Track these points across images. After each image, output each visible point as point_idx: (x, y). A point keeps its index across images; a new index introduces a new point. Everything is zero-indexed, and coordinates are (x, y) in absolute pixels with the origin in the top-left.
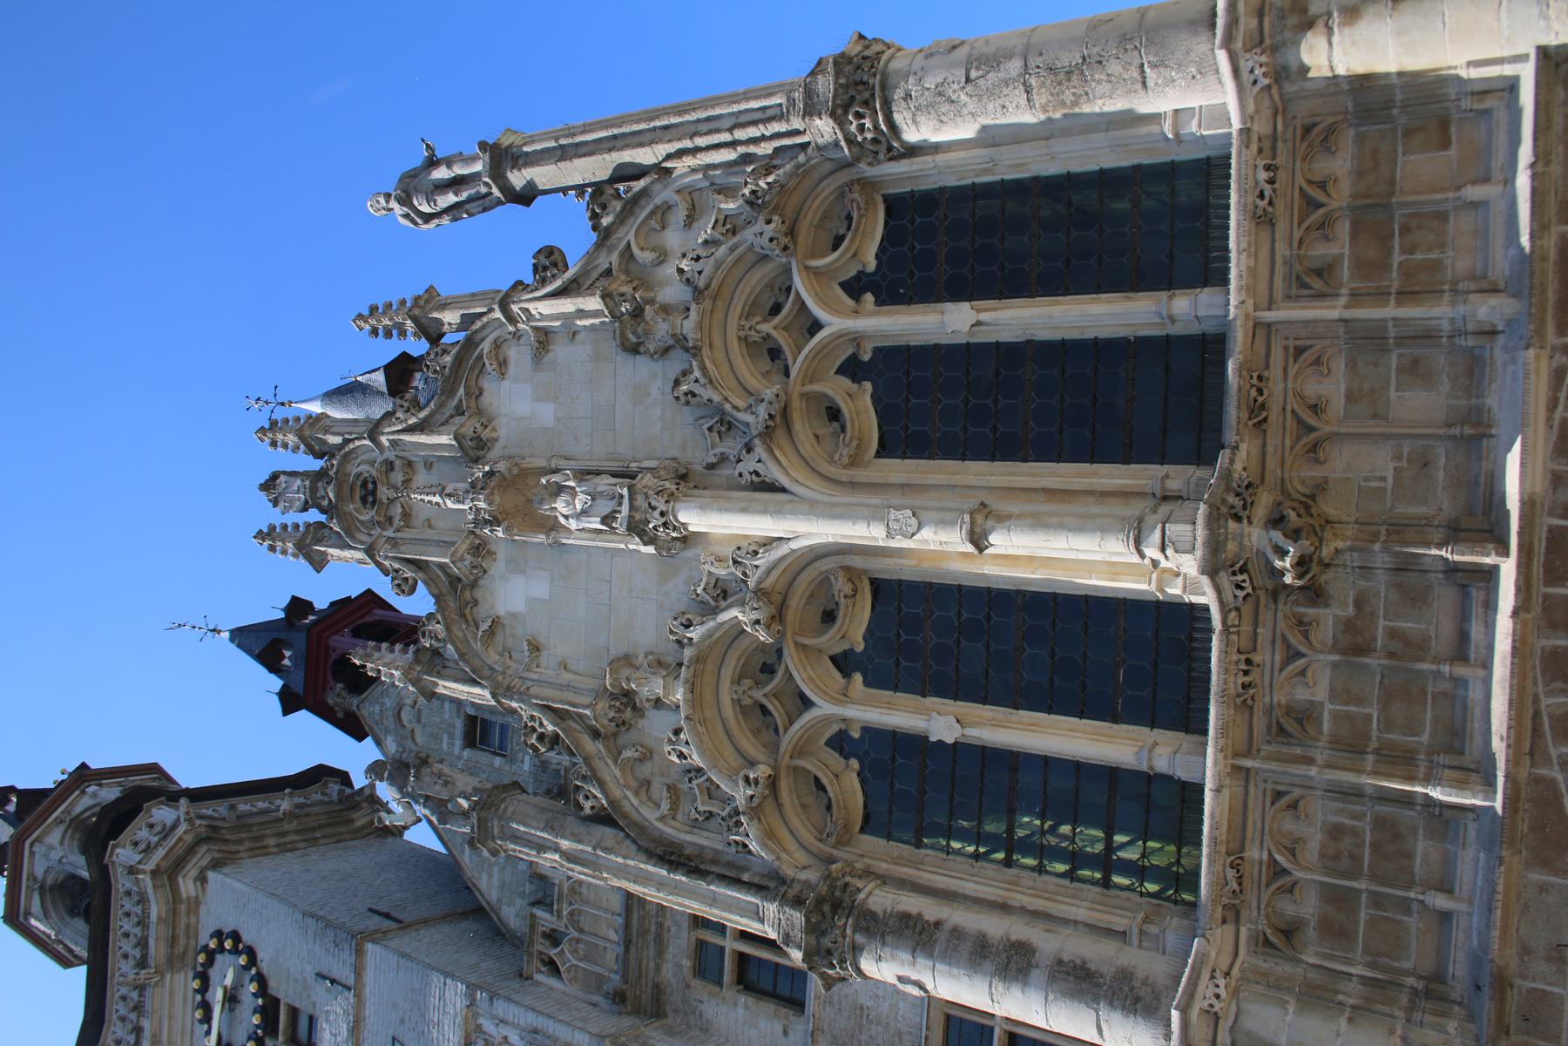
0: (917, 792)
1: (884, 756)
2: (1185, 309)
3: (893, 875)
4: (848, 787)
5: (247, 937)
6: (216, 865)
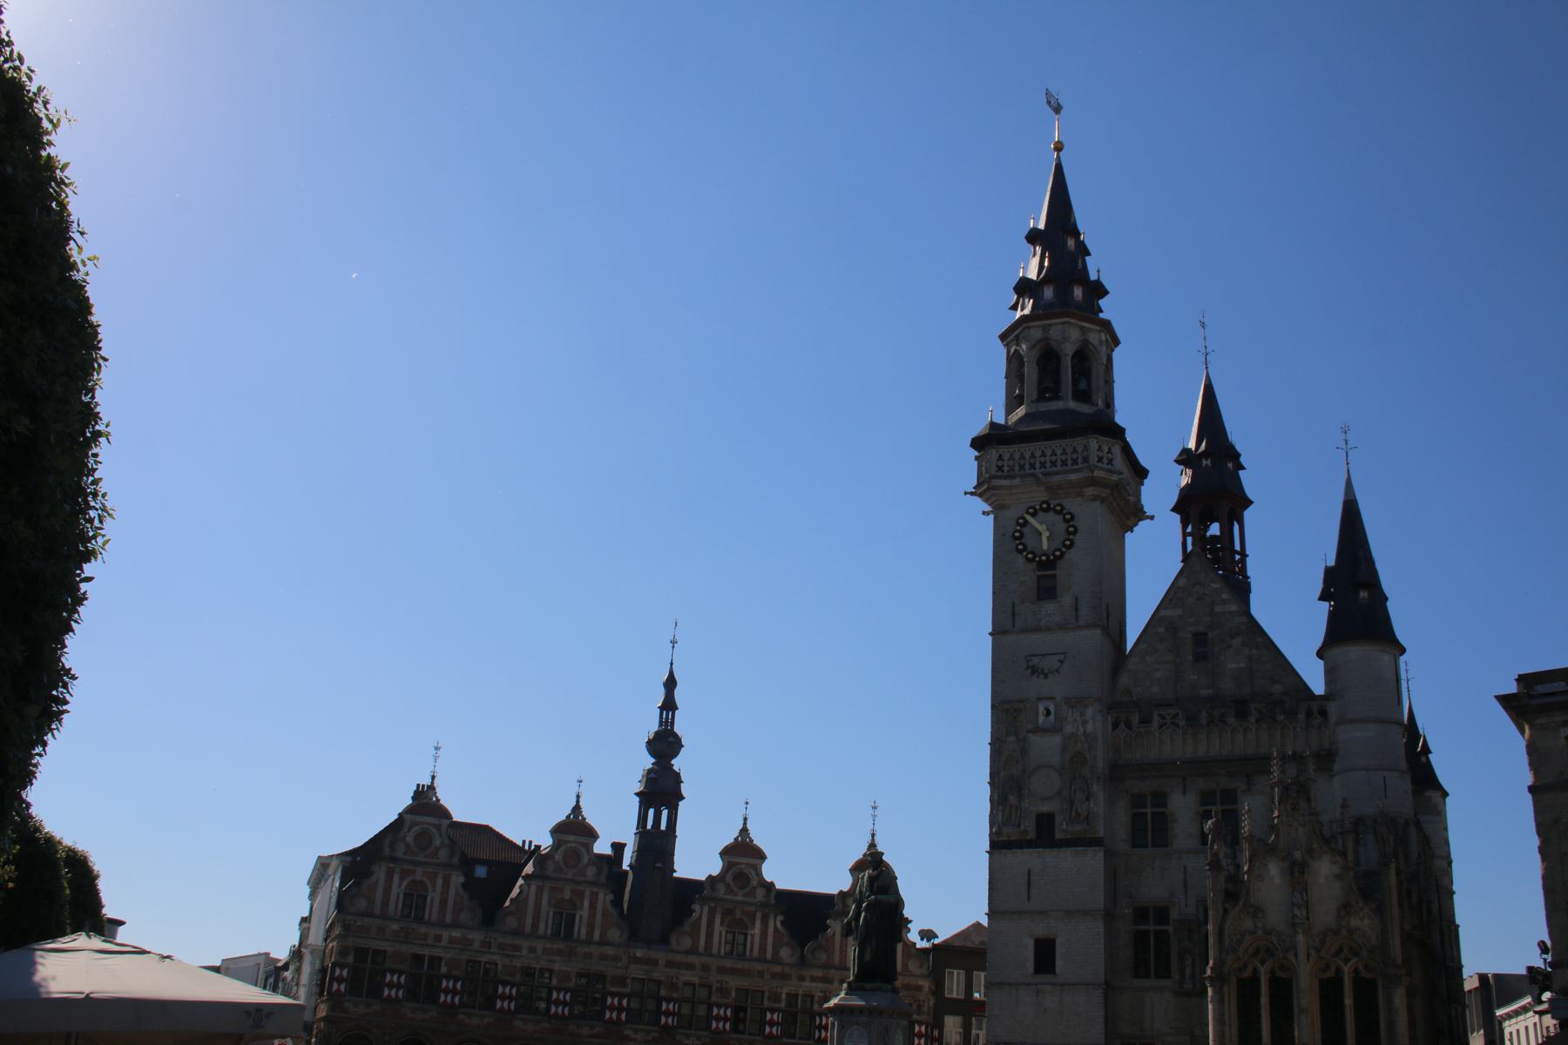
0: (1248, 988)
1: (1255, 979)
4: (1247, 974)
5: (1078, 539)
6: (1103, 500)
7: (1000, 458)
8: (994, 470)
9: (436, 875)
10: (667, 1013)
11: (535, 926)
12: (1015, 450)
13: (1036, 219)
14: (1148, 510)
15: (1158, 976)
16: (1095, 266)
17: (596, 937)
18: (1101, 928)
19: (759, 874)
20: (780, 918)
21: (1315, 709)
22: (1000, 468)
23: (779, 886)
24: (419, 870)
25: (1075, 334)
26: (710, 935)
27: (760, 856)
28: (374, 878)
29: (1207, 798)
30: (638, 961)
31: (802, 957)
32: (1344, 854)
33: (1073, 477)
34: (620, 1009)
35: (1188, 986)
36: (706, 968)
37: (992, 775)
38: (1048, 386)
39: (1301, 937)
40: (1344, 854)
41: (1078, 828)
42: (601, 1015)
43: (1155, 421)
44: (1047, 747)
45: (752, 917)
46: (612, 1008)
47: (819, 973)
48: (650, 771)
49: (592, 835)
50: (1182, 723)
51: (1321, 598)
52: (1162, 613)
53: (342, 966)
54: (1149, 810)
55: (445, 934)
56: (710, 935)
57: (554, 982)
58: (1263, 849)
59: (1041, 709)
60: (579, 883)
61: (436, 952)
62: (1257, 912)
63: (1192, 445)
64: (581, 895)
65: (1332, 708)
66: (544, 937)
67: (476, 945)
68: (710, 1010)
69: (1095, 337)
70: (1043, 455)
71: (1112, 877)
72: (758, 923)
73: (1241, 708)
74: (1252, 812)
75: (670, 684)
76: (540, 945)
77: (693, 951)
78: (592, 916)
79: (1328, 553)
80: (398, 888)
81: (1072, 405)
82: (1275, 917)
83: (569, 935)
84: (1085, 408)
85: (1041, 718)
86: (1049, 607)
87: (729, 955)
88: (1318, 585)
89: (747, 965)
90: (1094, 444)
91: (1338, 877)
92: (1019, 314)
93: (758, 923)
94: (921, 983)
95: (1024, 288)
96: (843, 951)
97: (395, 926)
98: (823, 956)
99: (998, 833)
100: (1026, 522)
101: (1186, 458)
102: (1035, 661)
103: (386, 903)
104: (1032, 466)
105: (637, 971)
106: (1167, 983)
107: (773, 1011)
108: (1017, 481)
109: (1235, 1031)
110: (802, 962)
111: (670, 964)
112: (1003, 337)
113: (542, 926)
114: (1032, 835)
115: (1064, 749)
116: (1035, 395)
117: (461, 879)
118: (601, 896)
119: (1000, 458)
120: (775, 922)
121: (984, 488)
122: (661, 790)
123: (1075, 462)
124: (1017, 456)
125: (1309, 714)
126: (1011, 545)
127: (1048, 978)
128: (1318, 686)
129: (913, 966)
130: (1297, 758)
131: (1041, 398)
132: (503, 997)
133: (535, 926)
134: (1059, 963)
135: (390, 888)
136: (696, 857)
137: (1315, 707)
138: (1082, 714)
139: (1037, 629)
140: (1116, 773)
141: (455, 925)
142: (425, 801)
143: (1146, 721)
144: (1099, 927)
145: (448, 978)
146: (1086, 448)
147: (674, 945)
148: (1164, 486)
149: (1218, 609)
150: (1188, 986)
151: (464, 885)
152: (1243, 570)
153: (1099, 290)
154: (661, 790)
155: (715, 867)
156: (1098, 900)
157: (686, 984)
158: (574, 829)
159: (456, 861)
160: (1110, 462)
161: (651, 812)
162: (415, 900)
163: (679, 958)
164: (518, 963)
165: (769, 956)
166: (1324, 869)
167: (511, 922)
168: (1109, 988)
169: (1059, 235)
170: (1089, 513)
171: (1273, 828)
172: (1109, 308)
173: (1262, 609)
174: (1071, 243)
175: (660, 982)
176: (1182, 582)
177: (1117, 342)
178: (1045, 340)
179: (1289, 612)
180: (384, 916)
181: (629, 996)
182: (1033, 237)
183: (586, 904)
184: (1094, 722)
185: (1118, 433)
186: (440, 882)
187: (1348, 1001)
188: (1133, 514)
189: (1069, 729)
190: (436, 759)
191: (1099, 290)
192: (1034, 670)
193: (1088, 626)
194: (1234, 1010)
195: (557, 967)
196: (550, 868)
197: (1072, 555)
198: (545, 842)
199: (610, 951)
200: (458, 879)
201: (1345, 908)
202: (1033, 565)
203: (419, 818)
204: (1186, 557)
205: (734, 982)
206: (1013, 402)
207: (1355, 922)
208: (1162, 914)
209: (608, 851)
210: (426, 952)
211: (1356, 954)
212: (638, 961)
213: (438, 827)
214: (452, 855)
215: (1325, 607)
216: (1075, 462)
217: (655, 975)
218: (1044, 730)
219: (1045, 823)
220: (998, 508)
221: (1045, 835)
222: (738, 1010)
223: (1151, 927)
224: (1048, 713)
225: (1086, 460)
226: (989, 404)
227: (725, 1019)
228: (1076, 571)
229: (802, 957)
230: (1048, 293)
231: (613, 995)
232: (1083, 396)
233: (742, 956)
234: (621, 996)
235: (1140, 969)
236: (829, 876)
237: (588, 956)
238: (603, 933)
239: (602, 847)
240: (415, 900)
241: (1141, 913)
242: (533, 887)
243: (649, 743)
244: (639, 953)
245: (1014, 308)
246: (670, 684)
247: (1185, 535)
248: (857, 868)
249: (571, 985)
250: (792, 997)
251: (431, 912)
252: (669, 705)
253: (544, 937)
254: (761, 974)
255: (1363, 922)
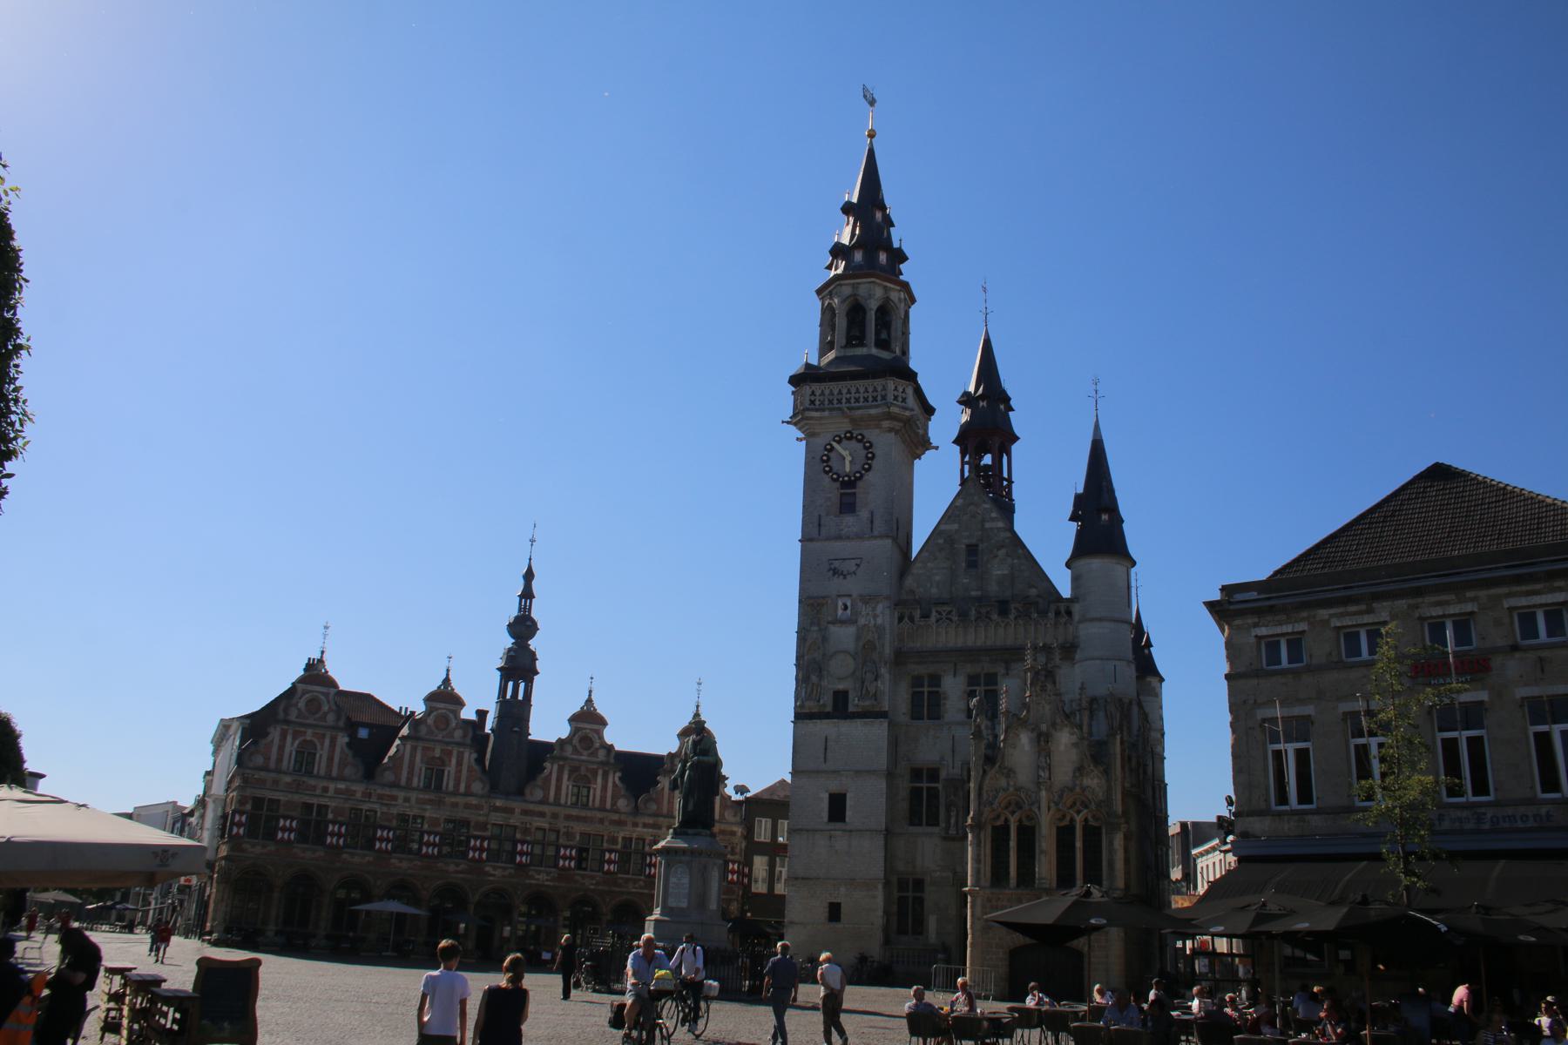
0: (1000, 834)
1: (1006, 827)
2: (1079, 882)
3: (987, 835)
4: (999, 823)
5: (874, 463)
6: (897, 432)
7: (813, 393)
8: (807, 404)
9: (323, 736)
10: (522, 853)
11: (409, 779)
12: (827, 387)
13: (850, 194)
14: (934, 441)
15: (928, 824)
16: (897, 236)
17: (462, 788)
18: (884, 785)
19: (601, 738)
20: (618, 774)
21: (1062, 608)
22: (812, 402)
23: (618, 747)
24: (309, 731)
25: (879, 292)
26: (558, 788)
27: (604, 723)
28: (270, 738)
29: (973, 680)
30: (496, 809)
31: (636, 807)
32: (1080, 727)
33: (873, 412)
34: (481, 850)
35: (952, 832)
36: (555, 816)
37: (798, 659)
38: (855, 335)
39: (1043, 793)
40: (1080, 727)
41: (867, 703)
42: (464, 855)
43: (942, 367)
44: (843, 636)
45: (595, 774)
46: (475, 849)
47: (650, 821)
48: (510, 650)
49: (459, 703)
50: (955, 618)
51: (1071, 519)
52: (942, 527)
53: (241, 813)
54: (926, 689)
55: (332, 786)
56: (558, 788)
57: (426, 827)
58: (1016, 722)
59: (840, 603)
60: (448, 743)
61: (323, 801)
62: (1009, 773)
63: (971, 389)
64: (450, 753)
65: (1076, 609)
66: (417, 789)
67: (359, 795)
68: (558, 851)
69: (894, 296)
70: (849, 392)
71: (894, 743)
72: (599, 780)
73: (1003, 607)
74: (1009, 691)
75: (529, 576)
76: (413, 796)
77: (541, 802)
78: (459, 771)
79: (1077, 481)
80: (291, 746)
81: (874, 351)
82: (1024, 777)
83: (439, 788)
84: (885, 355)
85: (840, 612)
86: (849, 520)
87: (574, 805)
88: (1069, 508)
89: (589, 814)
90: (891, 384)
91: (1075, 745)
92: (833, 273)
93: (599, 780)
94: (735, 829)
95: (838, 251)
96: (671, 803)
97: (288, 779)
98: (654, 807)
99: (802, 706)
100: (832, 448)
101: (966, 400)
102: (836, 564)
103: (280, 760)
104: (840, 401)
105: (496, 818)
106: (936, 830)
107: (611, 851)
108: (826, 413)
109: (988, 868)
110: (636, 811)
111: (525, 812)
112: (819, 292)
113: (415, 782)
114: (829, 709)
115: (858, 638)
116: (844, 342)
117: (346, 739)
118: (466, 755)
119: (813, 393)
120: (615, 778)
121: (799, 418)
122: (519, 666)
123: (875, 399)
124: (827, 392)
125: (1058, 613)
126: (820, 465)
127: (839, 825)
128: (1065, 590)
129: (729, 815)
130: (1047, 649)
131: (849, 344)
132: (381, 840)
133: (409, 779)
134: (848, 813)
135: (283, 746)
136: (548, 723)
137: (1062, 608)
138: (874, 609)
139: (839, 538)
140: (900, 658)
141: (341, 778)
142: (315, 673)
143: (926, 616)
144: (882, 784)
145: (334, 823)
146: (884, 389)
147: (528, 797)
148: (947, 422)
149: (988, 525)
150: (952, 832)
151: (349, 745)
152: (1009, 493)
153: (899, 256)
154: (519, 666)
155: (564, 731)
156: (882, 762)
157: (538, 829)
158: (444, 698)
159: (341, 724)
160: (904, 400)
161: (510, 684)
162: (305, 758)
163: (531, 807)
164: (394, 811)
165: (608, 806)
166: (1064, 739)
167: (389, 776)
168: (888, 833)
169: (869, 207)
170: (885, 442)
171: (1025, 706)
172: (908, 271)
173: (1022, 526)
174: (879, 215)
175: (515, 827)
176: (960, 502)
177: (913, 301)
178: (854, 295)
179: (1046, 532)
180: (278, 771)
181: (489, 839)
182: (848, 209)
183: (454, 761)
184: (883, 615)
185: (911, 376)
186: (327, 742)
187: (1079, 844)
188: (920, 444)
189: (862, 621)
190: (325, 636)
191: (899, 256)
192: (835, 572)
193: (881, 537)
194: (988, 851)
195: (427, 814)
196: (423, 730)
197: (869, 477)
198: (419, 708)
199: (474, 801)
200: (343, 739)
201: (1080, 770)
202: (837, 485)
203: (310, 687)
204: (963, 482)
205: (578, 828)
206: (825, 347)
207: (1087, 782)
208: (933, 774)
209: (473, 717)
210: (315, 801)
211: (1086, 807)
212: (496, 809)
213: (326, 695)
214: (338, 719)
215: (1074, 526)
216: (875, 399)
217: (512, 821)
218: (842, 622)
219: (841, 698)
220: (810, 436)
221: (840, 708)
222: (581, 850)
223: (925, 785)
224: (846, 608)
225: (884, 398)
226: (806, 349)
227: (571, 858)
228: (872, 491)
229: (636, 807)
230: (858, 256)
231: (476, 837)
232: (883, 344)
233: (585, 806)
234: (483, 839)
235: (914, 819)
236: (662, 741)
237: (455, 805)
238: (468, 786)
239: (468, 714)
240: (305, 758)
241: (916, 774)
242: (408, 747)
243: (509, 625)
244: (498, 803)
245: (829, 267)
246: (529, 576)
247: (963, 463)
248: (684, 734)
249: (440, 829)
250: (627, 840)
251: (320, 766)
252: (527, 594)
253: (417, 789)
254: (601, 821)
255: (1093, 781)
